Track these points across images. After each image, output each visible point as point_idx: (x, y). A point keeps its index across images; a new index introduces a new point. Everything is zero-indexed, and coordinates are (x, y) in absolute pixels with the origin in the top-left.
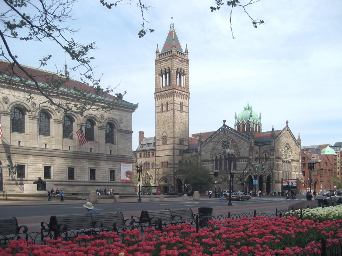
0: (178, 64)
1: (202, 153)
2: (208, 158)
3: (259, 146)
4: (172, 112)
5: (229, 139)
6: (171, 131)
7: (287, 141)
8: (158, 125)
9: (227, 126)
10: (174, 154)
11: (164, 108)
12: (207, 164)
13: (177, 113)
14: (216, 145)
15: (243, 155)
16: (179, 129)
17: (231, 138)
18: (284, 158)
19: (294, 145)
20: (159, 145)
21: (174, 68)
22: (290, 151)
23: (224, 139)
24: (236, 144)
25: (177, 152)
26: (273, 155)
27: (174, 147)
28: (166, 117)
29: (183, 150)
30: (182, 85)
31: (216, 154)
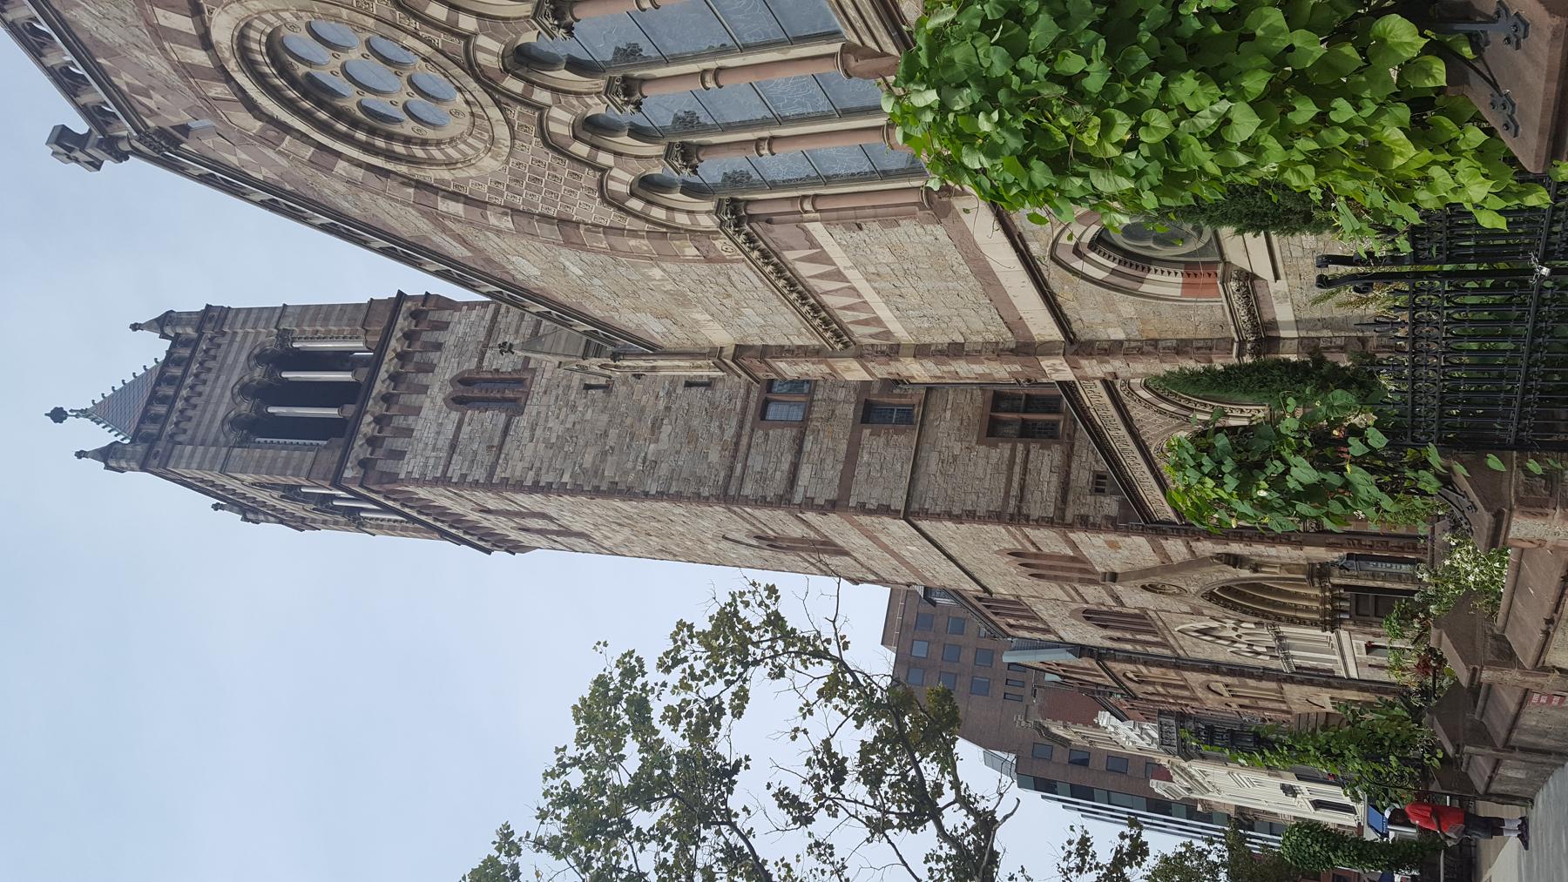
0: (208, 416)
16: (656, 426)
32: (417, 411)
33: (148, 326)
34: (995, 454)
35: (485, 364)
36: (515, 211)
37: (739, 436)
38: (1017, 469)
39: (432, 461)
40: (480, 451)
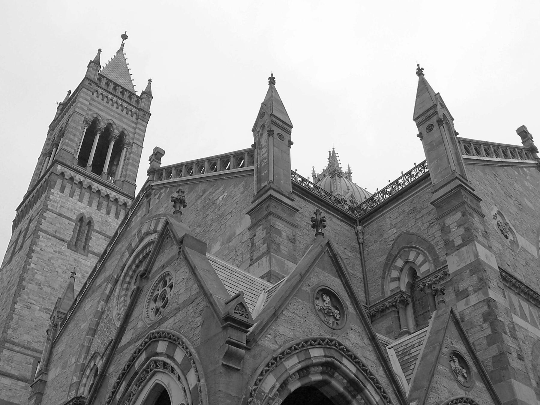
0: (102, 107)
32: (81, 200)
33: (149, 88)
36: (103, 313)
37: (33, 350)
39: (56, 205)
40: (55, 227)
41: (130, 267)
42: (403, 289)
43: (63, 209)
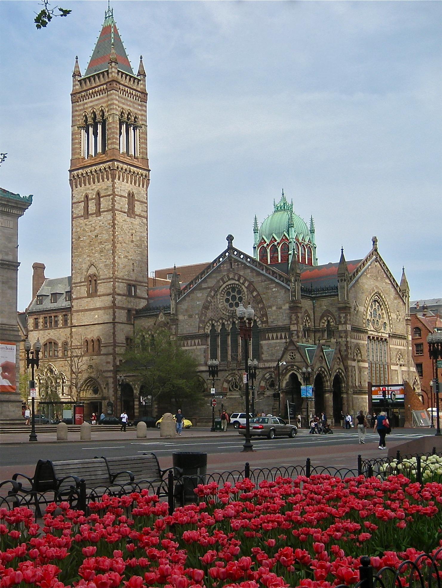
1: (181, 317)
2: (194, 330)
3: (312, 299)
4: (109, 216)
5: (241, 281)
6: (108, 262)
7: (377, 287)
8: (77, 248)
9: (236, 250)
10: (114, 319)
11: (92, 207)
12: (191, 346)
13: (121, 218)
14: (213, 297)
15: (276, 323)
16: (126, 257)
17: (246, 280)
18: (372, 329)
19: (392, 297)
20: (80, 298)
21: (114, 112)
22: (384, 311)
23: (229, 282)
24: (258, 294)
25: (122, 316)
26: (345, 323)
27: (113, 302)
28: (95, 229)
29: (136, 310)
30: (132, 152)
31: (212, 320)
32: (127, 183)
33: (141, 66)
34: (124, 340)
35: (136, 202)
38: (122, 345)
41: (224, 289)
42: (325, 326)
43: (122, 192)
